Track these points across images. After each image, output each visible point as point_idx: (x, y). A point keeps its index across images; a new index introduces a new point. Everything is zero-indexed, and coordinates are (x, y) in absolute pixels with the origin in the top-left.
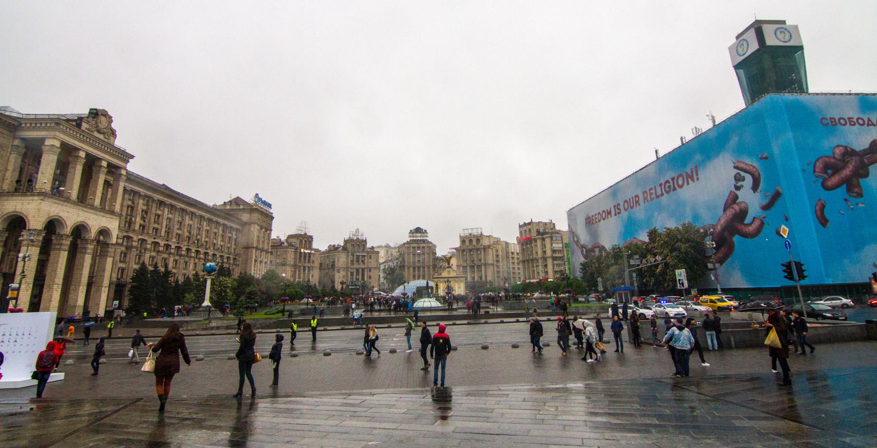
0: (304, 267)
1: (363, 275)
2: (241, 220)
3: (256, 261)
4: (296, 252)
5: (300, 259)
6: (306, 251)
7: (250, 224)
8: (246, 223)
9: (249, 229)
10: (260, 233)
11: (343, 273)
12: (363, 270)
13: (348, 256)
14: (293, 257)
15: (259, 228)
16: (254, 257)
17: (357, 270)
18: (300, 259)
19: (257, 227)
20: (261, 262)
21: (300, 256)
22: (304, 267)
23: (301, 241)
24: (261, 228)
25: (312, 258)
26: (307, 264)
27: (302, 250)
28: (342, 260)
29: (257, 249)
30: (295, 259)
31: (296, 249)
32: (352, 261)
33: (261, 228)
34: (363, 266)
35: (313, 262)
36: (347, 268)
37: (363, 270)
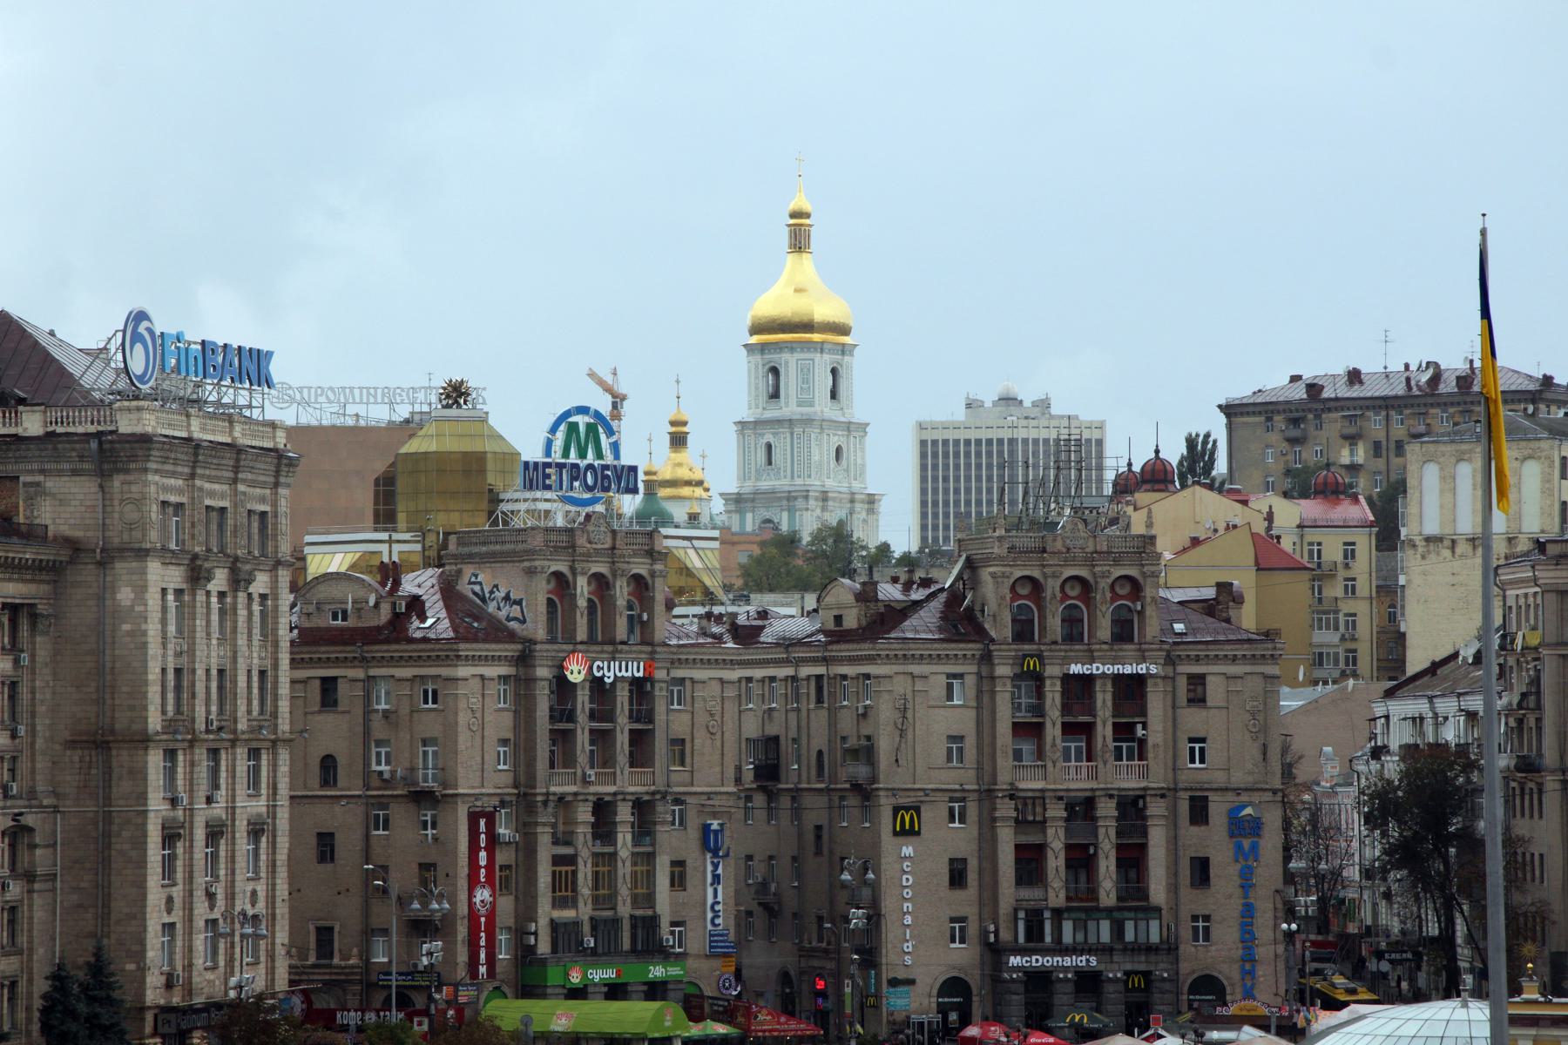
0: (603, 810)
1: (1132, 859)
2: (34, 534)
3: (170, 837)
4: (521, 684)
5: (562, 738)
6: (610, 672)
7: (107, 557)
8: (75, 548)
9: (103, 595)
10: (186, 614)
11: (948, 837)
12: (1132, 808)
13: (986, 681)
14: (500, 721)
15: (174, 577)
16: (157, 804)
17: (1082, 809)
18: (562, 738)
19: (162, 576)
20: (215, 833)
21: (563, 710)
22: (603, 810)
23: (562, 583)
24: (197, 576)
25: (670, 719)
26: (627, 782)
27: (576, 673)
28: (928, 715)
29: (180, 736)
30: (520, 745)
31: (524, 659)
32: (1029, 730)
33: (197, 576)
34: (1128, 780)
35: (679, 747)
36: (987, 795)
37: (1132, 808)
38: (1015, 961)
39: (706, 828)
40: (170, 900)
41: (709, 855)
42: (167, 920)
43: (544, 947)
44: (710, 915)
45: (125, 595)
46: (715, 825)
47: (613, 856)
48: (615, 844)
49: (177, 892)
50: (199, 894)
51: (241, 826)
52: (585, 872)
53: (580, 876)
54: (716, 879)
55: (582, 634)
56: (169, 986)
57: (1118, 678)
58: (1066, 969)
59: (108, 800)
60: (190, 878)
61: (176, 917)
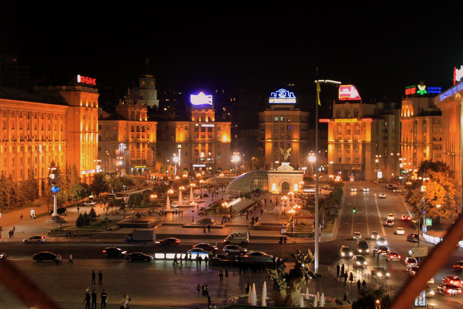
38: (194, 166)
39: (152, 147)
40: (83, 156)
41: (152, 151)
42: (83, 158)
43: (130, 163)
44: (152, 159)
45: (77, 113)
46: (153, 147)
47: (139, 151)
48: (139, 148)
49: (84, 154)
50: (87, 155)
51: (92, 145)
52: (136, 153)
53: (135, 153)
54: (153, 154)
55: (135, 119)
56: (83, 167)
57: (208, 127)
58: (201, 167)
59: (75, 141)
60: (86, 153)
61: (84, 158)
